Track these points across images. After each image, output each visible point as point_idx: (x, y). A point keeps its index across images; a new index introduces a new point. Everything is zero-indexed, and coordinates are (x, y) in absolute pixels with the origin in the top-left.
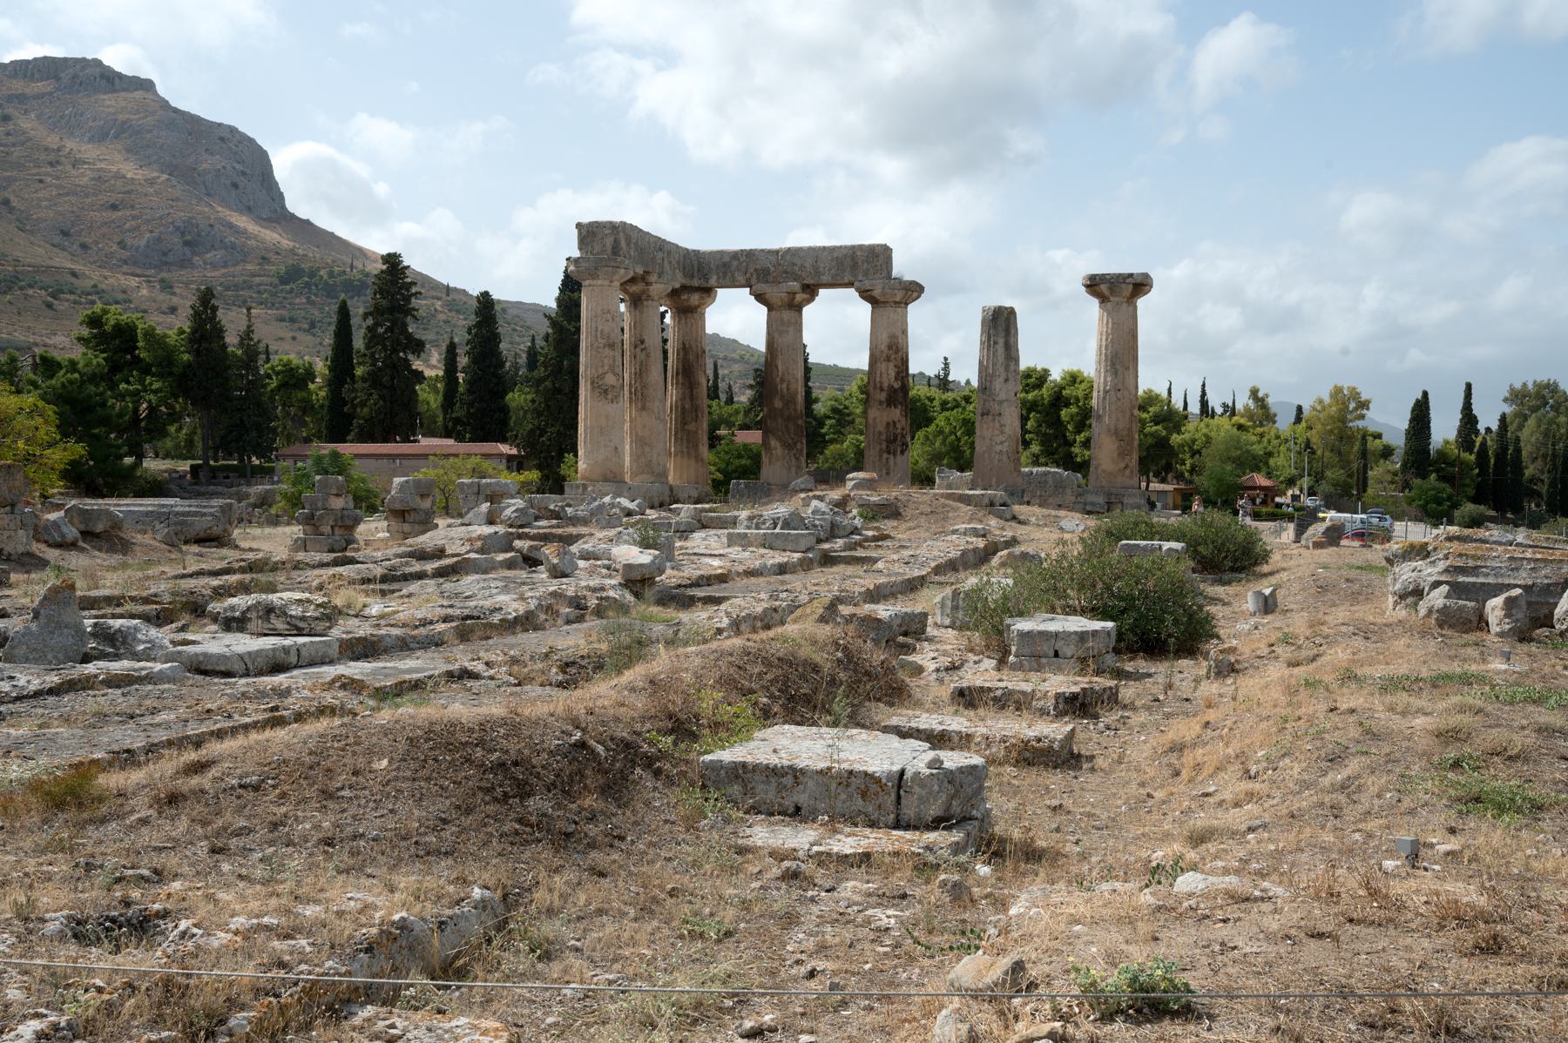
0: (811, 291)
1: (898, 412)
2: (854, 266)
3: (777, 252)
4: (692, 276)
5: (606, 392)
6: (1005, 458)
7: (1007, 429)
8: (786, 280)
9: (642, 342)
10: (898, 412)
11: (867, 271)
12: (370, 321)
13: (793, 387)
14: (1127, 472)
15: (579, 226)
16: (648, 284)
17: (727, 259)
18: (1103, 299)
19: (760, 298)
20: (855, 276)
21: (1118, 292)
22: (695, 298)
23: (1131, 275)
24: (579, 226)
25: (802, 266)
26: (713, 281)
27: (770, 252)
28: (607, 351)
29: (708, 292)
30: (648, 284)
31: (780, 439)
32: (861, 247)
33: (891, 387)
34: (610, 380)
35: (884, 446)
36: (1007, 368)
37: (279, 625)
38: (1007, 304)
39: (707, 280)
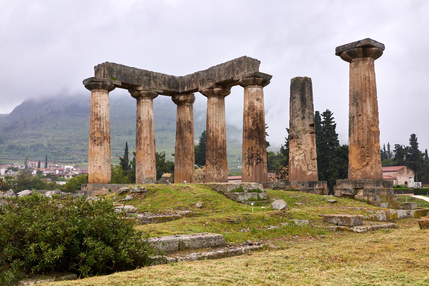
1: (254, 142)
2: (233, 70)
3: (207, 70)
4: (178, 88)
5: (95, 141)
9: (140, 118)
13: (215, 134)
16: (139, 91)
17: (190, 78)
20: (234, 75)
22: (182, 98)
23: (359, 42)
31: (209, 160)
33: (251, 129)
35: (247, 161)
36: (303, 112)
38: (309, 76)
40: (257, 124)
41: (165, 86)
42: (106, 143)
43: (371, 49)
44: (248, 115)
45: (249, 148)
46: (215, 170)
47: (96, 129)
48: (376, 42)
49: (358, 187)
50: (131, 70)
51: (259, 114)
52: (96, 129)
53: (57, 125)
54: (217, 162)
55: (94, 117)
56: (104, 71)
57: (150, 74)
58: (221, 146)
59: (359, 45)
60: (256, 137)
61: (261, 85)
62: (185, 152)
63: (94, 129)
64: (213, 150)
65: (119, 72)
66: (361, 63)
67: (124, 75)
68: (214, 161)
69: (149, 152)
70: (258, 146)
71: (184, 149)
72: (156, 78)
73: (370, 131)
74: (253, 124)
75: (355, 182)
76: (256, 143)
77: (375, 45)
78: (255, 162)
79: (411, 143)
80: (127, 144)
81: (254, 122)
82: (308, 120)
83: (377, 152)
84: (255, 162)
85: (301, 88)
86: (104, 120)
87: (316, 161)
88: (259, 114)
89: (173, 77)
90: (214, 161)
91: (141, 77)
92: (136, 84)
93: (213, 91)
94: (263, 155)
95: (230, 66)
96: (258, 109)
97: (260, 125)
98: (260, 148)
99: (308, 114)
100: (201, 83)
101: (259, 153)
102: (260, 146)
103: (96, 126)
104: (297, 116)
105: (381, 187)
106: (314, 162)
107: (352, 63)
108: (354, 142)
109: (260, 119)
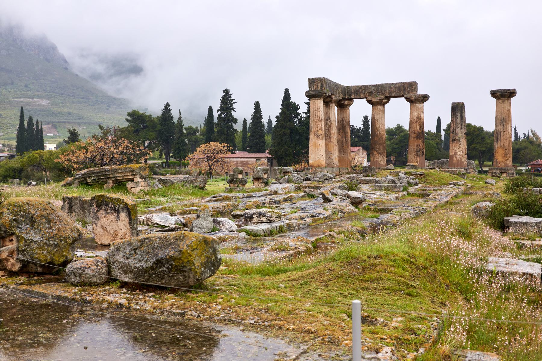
0: (388, 99)
2: (404, 90)
8: (379, 95)
9: (330, 119)
11: (408, 92)
12: (220, 112)
15: (309, 79)
18: (498, 98)
19: (369, 102)
20: (405, 93)
21: (503, 96)
22: (346, 102)
23: (509, 90)
24: (309, 79)
25: (385, 91)
26: (353, 97)
27: (373, 86)
29: (351, 100)
31: (377, 151)
32: (406, 83)
35: (416, 153)
37: (264, 219)
59: (509, 92)
64: (380, 144)
66: (506, 101)
74: (420, 129)
79: (364, 125)
80: (22, 108)
81: (420, 127)
85: (458, 109)
95: (400, 86)
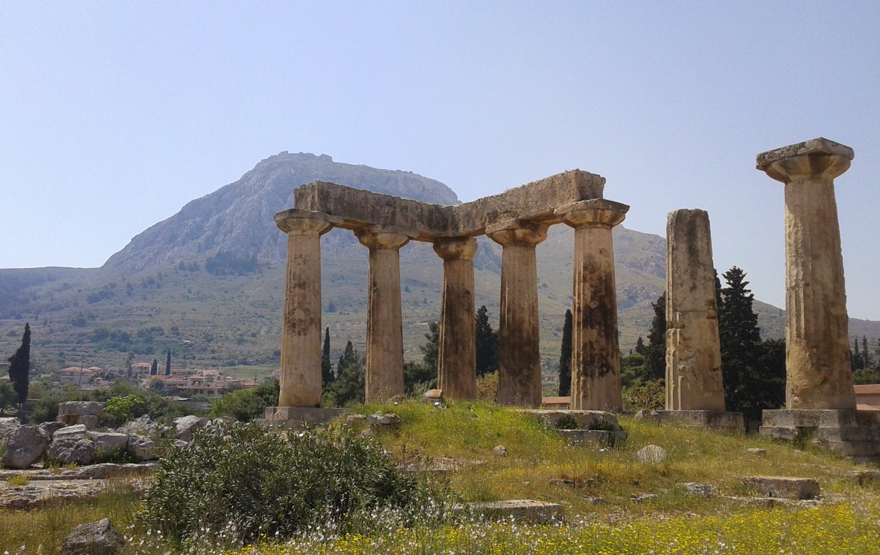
1: (595, 332)
3: (502, 195)
4: (445, 228)
5: (294, 326)
6: (690, 376)
7: (694, 343)
10: (595, 332)
13: (517, 316)
14: (827, 387)
16: (374, 235)
22: (452, 248)
23: (803, 145)
28: (297, 290)
30: (374, 235)
34: (299, 315)
36: (693, 276)
39: (457, 229)
40: (600, 297)
41: (423, 223)
42: (313, 329)
43: (826, 157)
44: (585, 280)
45: (585, 345)
46: (518, 386)
47: (296, 305)
48: (838, 144)
49: (806, 424)
50: (362, 196)
51: (604, 278)
52: (296, 305)
53: (190, 292)
54: (521, 370)
55: (293, 282)
56: (313, 197)
57: (395, 203)
58: (529, 339)
59: (802, 150)
60: (599, 323)
61: (608, 225)
62: (457, 349)
63: (293, 303)
65: (340, 200)
66: (807, 185)
67: (349, 204)
68: (516, 367)
69: (391, 349)
70: (603, 341)
71: (457, 345)
72: (407, 208)
73: (828, 315)
74: (592, 299)
75: (801, 416)
76: (599, 334)
77: (833, 150)
78: (597, 372)
82: (703, 291)
83: (843, 355)
84: (597, 372)
86: (311, 287)
87: (720, 372)
88: (604, 278)
89: (437, 207)
90: (516, 367)
91: (378, 208)
92: (369, 221)
93: (514, 234)
94: (612, 357)
96: (603, 269)
97: (607, 300)
98: (607, 345)
99: (703, 281)
100: (490, 218)
101: (604, 353)
102: (607, 340)
103: (296, 298)
104: (682, 285)
105: (854, 424)
106: (717, 375)
107: (790, 184)
108: (799, 336)
109: (606, 289)
